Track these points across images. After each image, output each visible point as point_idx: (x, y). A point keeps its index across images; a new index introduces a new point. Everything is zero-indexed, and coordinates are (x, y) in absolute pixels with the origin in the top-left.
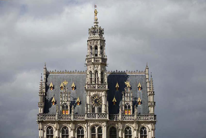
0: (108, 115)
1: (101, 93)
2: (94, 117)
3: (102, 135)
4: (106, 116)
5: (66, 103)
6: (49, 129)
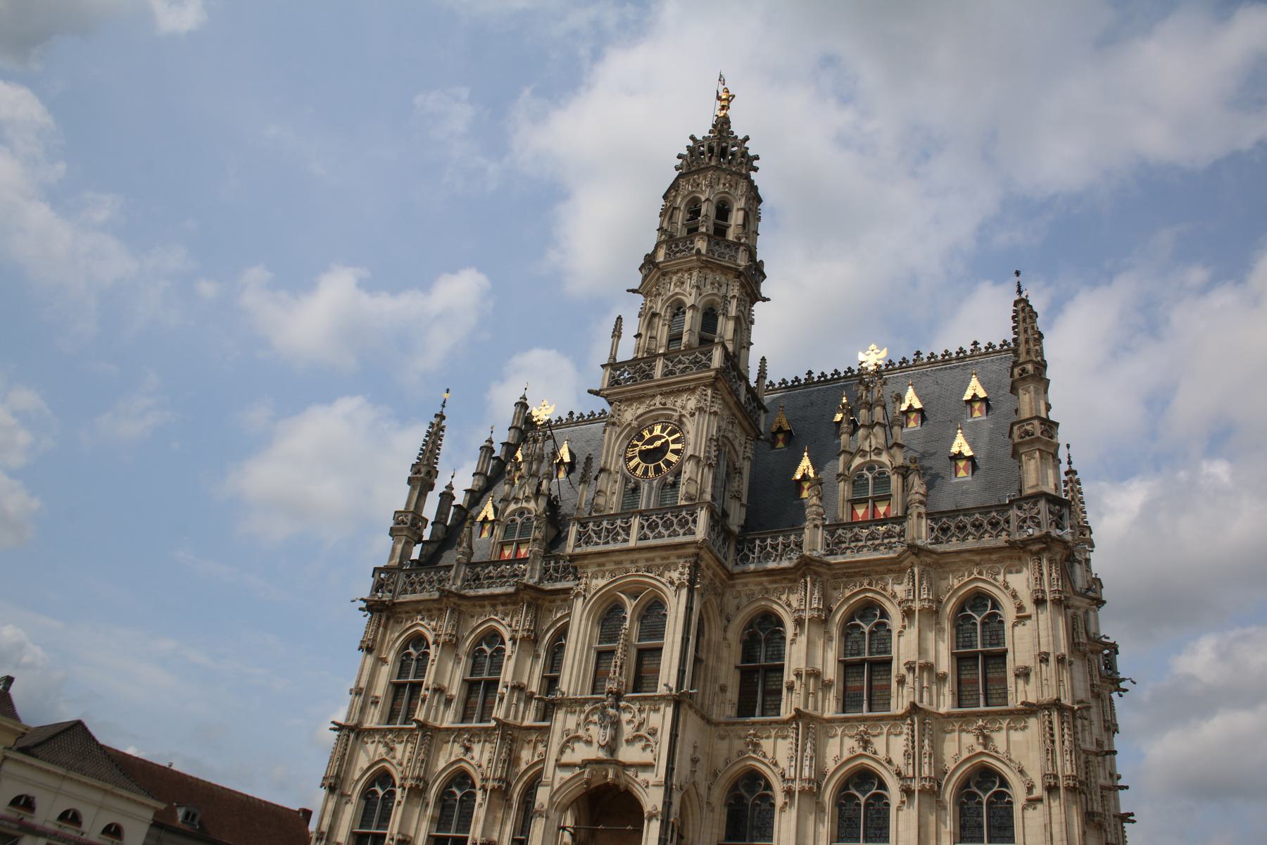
4: (690, 519)
5: (525, 505)
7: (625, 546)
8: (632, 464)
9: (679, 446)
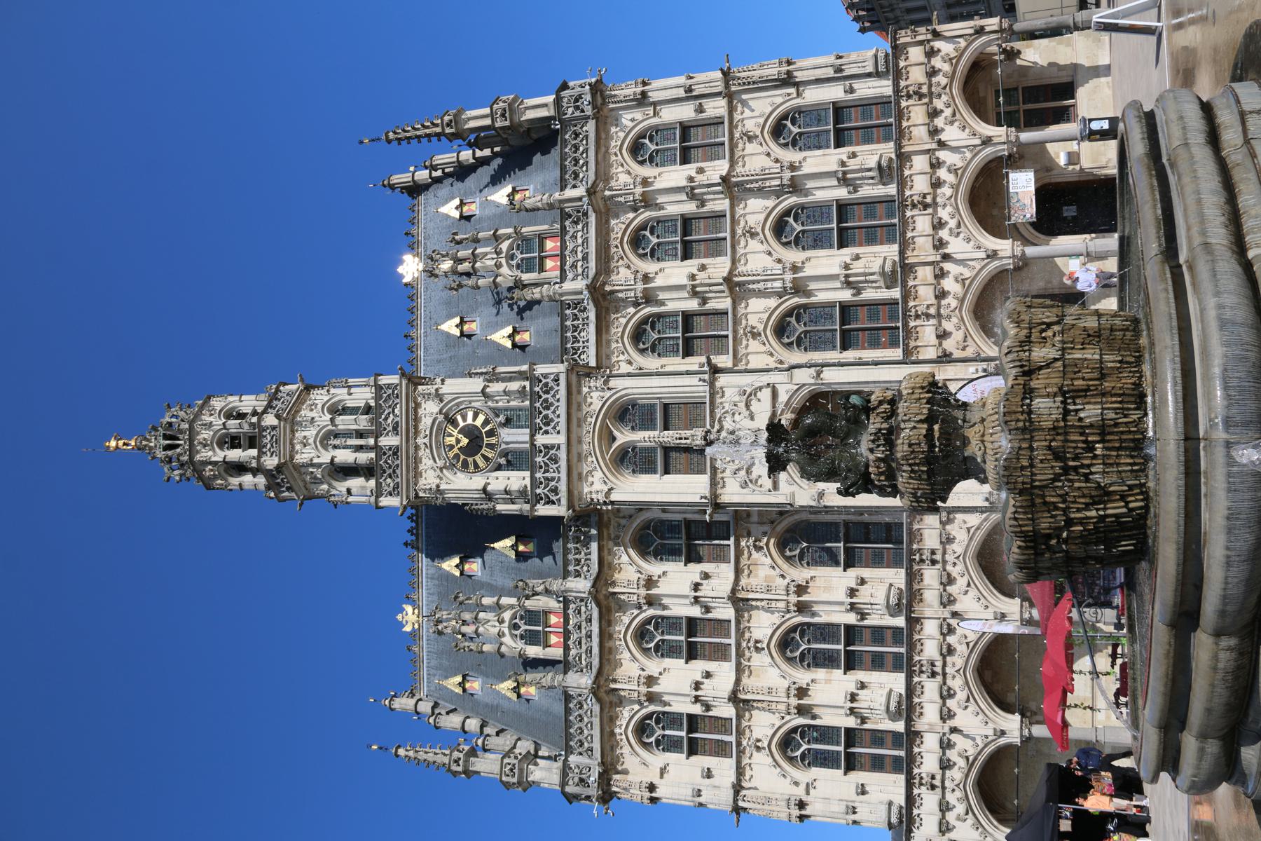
0: (541, 369)
1: (425, 423)
2: (555, 460)
3: (666, 407)
5: (506, 624)
6: (652, 739)
7: (564, 448)
8: (481, 463)
9: (470, 415)
